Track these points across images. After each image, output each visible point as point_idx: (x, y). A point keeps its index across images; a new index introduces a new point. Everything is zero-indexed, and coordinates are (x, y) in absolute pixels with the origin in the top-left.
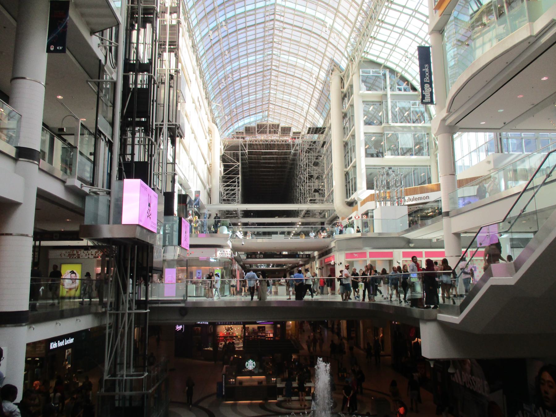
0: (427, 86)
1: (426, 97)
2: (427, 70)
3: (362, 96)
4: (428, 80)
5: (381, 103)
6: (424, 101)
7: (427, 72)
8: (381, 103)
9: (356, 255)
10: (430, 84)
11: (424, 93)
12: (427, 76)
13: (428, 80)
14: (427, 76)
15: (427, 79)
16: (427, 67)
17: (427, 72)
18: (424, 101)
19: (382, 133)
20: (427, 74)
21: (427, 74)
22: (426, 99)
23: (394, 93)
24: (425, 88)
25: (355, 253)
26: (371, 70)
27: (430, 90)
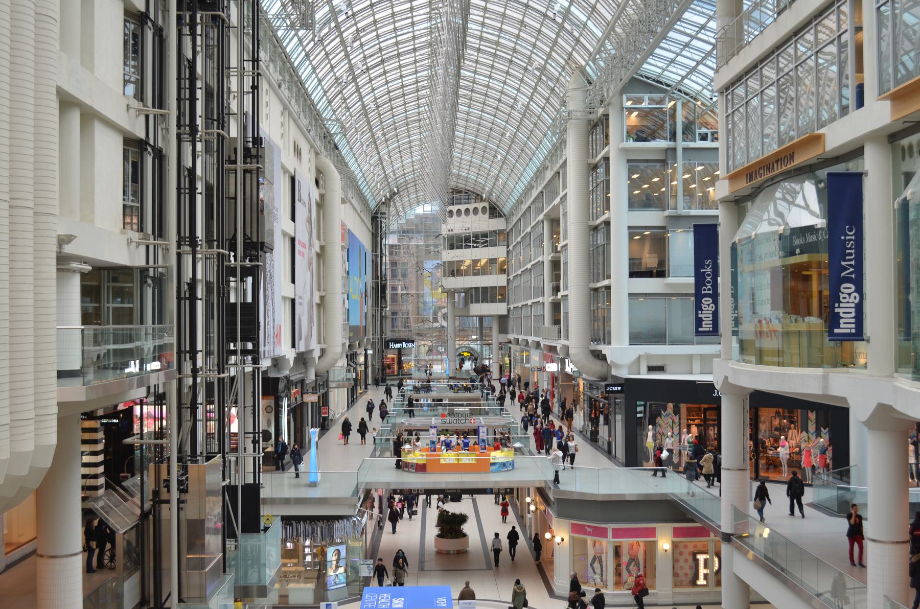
0: (707, 301)
1: (704, 323)
2: (709, 270)
3: (625, 151)
4: (709, 290)
5: (664, 162)
6: (700, 329)
7: (709, 275)
8: (664, 162)
9: (589, 530)
10: (715, 297)
11: (700, 316)
12: (709, 282)
13: (709, 290)
14: (709, 282)
15: (707, 289)
16: (708, 266)
17: (709, 275)
18: (700, 329)
19: (664, 228)
20: (709, 279)
21: (709, 279)
22: (704, 326)
23: (692, 145)
24: (703, 306)
25: (589, 527)
26: (646, 97)
27: (712, 308)
